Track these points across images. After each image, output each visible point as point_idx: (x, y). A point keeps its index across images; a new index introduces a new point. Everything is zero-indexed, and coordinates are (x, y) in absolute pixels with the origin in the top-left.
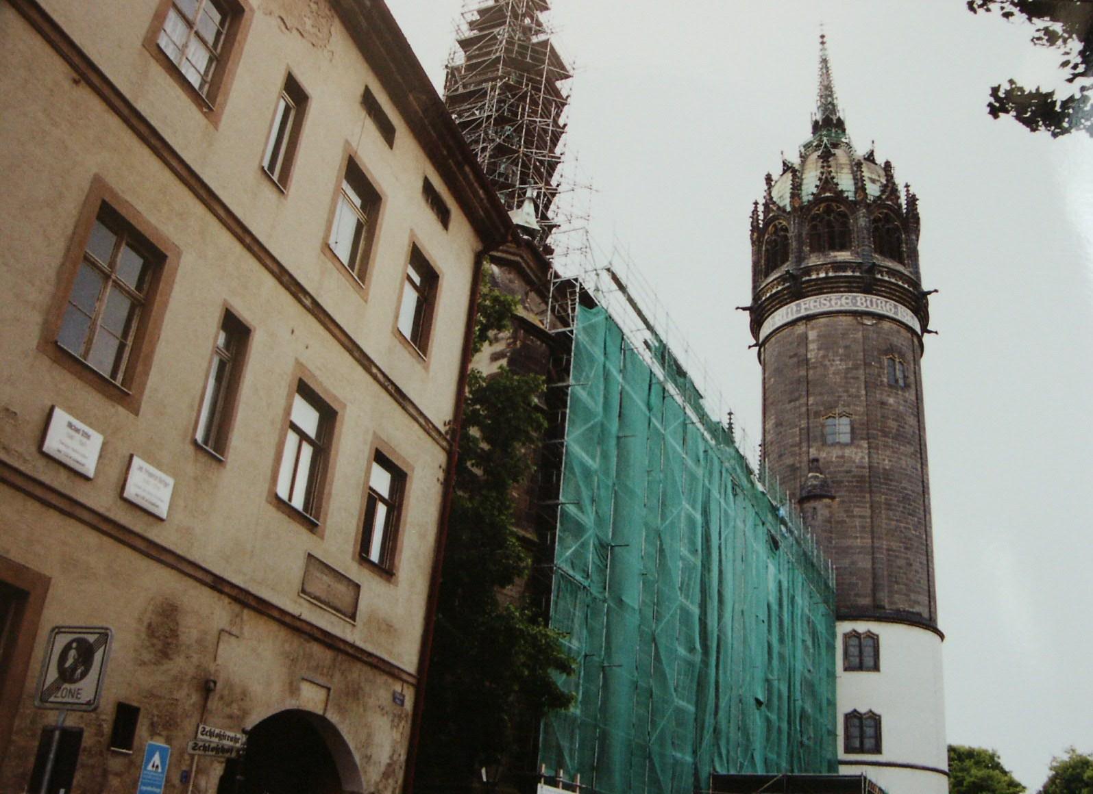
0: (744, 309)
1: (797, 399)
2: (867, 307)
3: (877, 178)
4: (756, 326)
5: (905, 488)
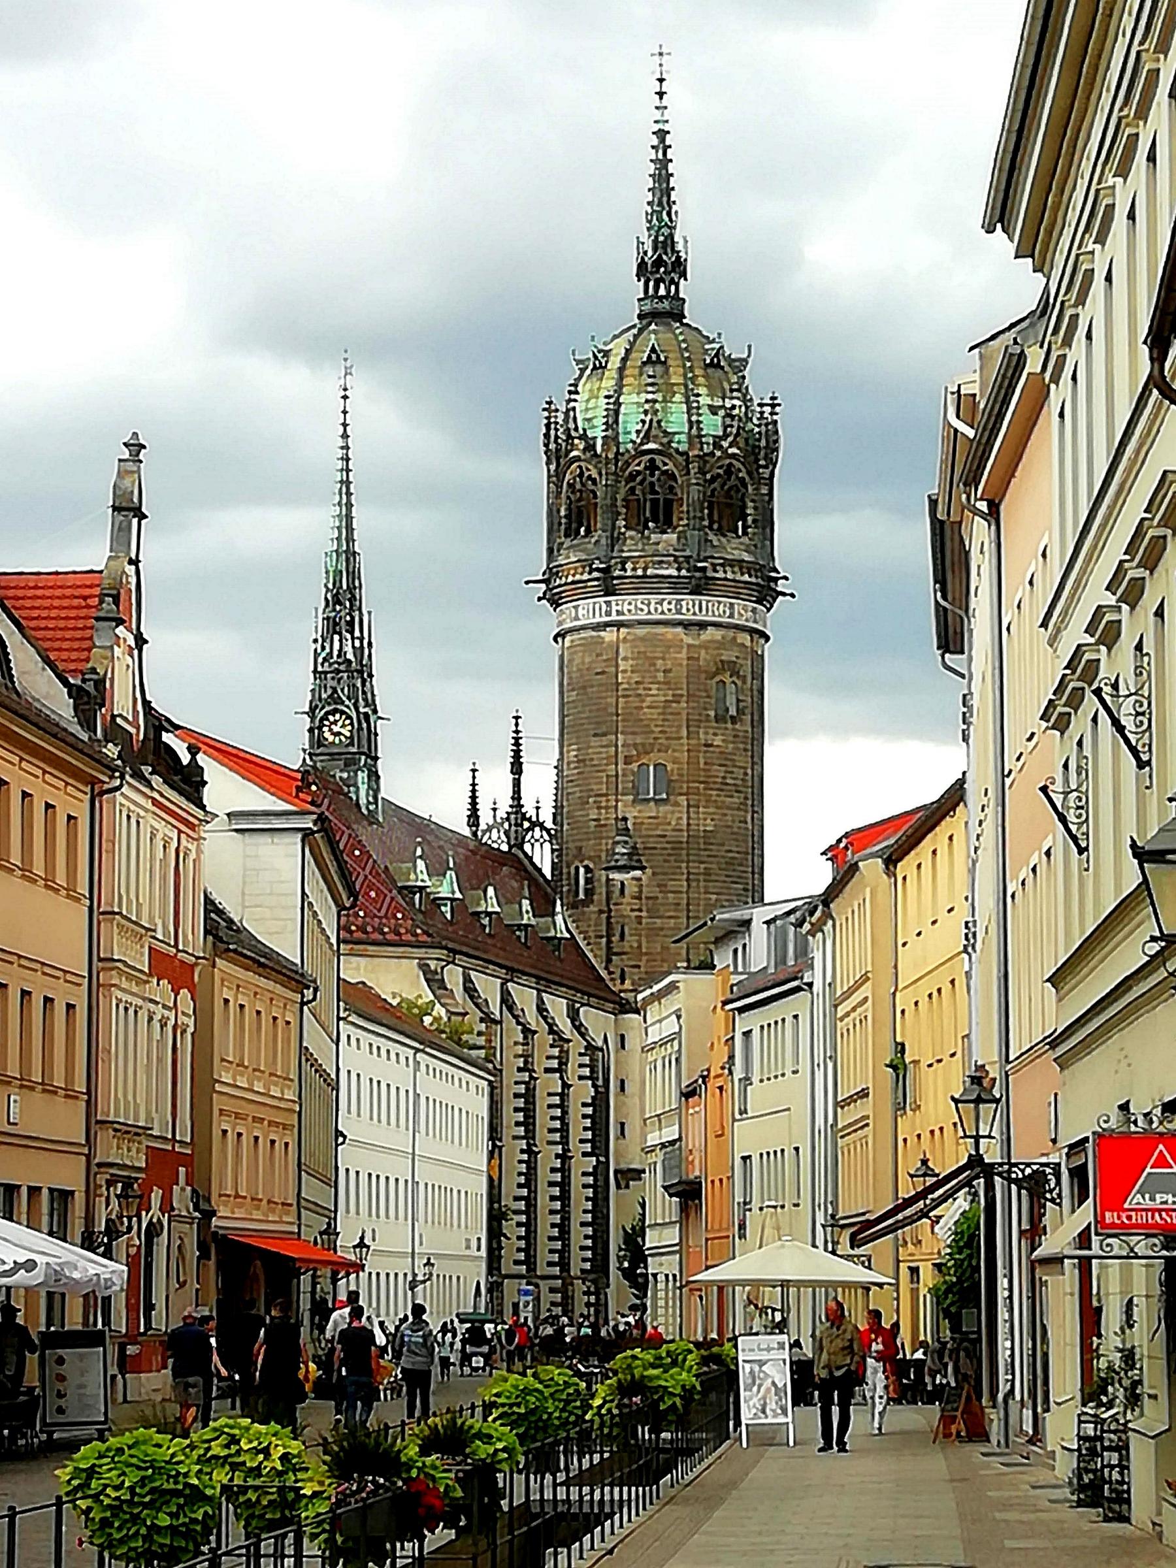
1: (604, 735)
2: (694, 614)
3: (721, 403)
5: (730, 851)
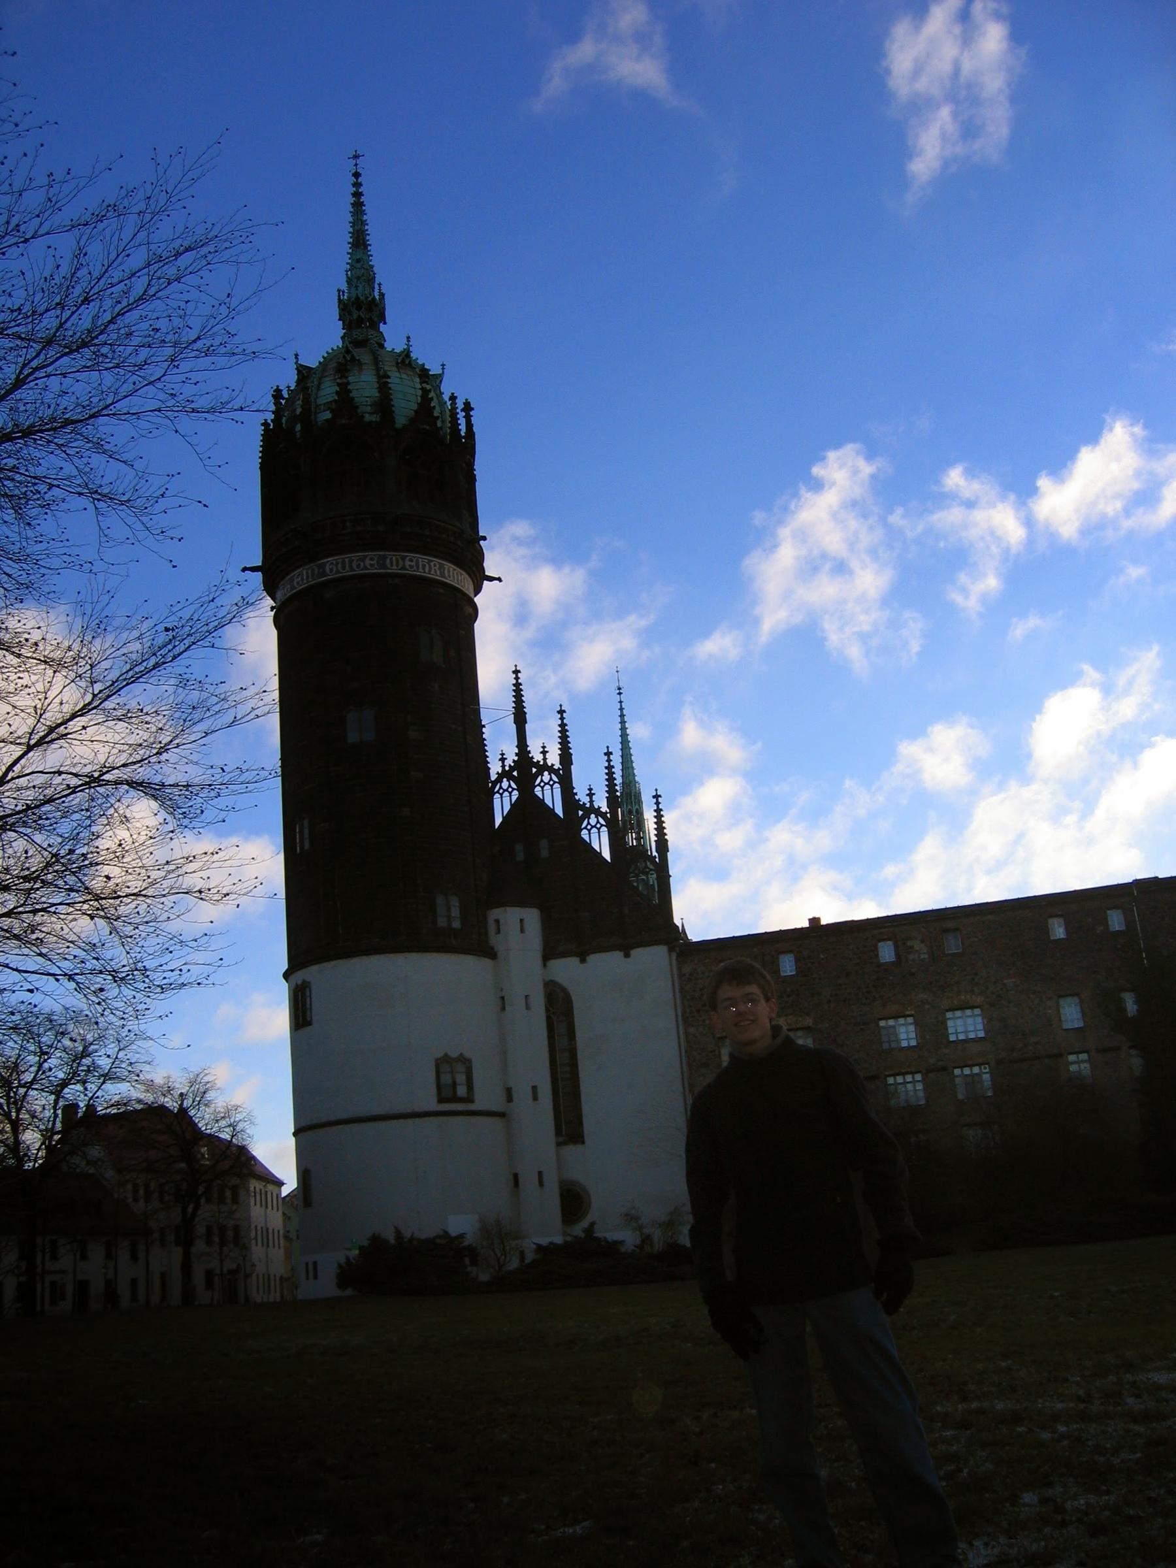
0: (254, 569)
4: (270, 588)
